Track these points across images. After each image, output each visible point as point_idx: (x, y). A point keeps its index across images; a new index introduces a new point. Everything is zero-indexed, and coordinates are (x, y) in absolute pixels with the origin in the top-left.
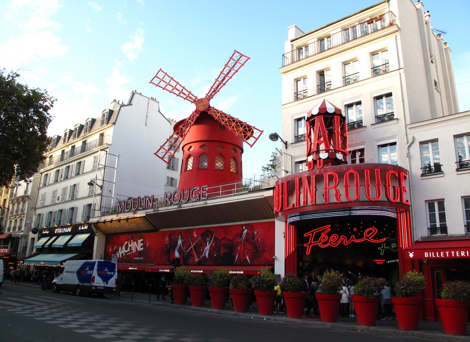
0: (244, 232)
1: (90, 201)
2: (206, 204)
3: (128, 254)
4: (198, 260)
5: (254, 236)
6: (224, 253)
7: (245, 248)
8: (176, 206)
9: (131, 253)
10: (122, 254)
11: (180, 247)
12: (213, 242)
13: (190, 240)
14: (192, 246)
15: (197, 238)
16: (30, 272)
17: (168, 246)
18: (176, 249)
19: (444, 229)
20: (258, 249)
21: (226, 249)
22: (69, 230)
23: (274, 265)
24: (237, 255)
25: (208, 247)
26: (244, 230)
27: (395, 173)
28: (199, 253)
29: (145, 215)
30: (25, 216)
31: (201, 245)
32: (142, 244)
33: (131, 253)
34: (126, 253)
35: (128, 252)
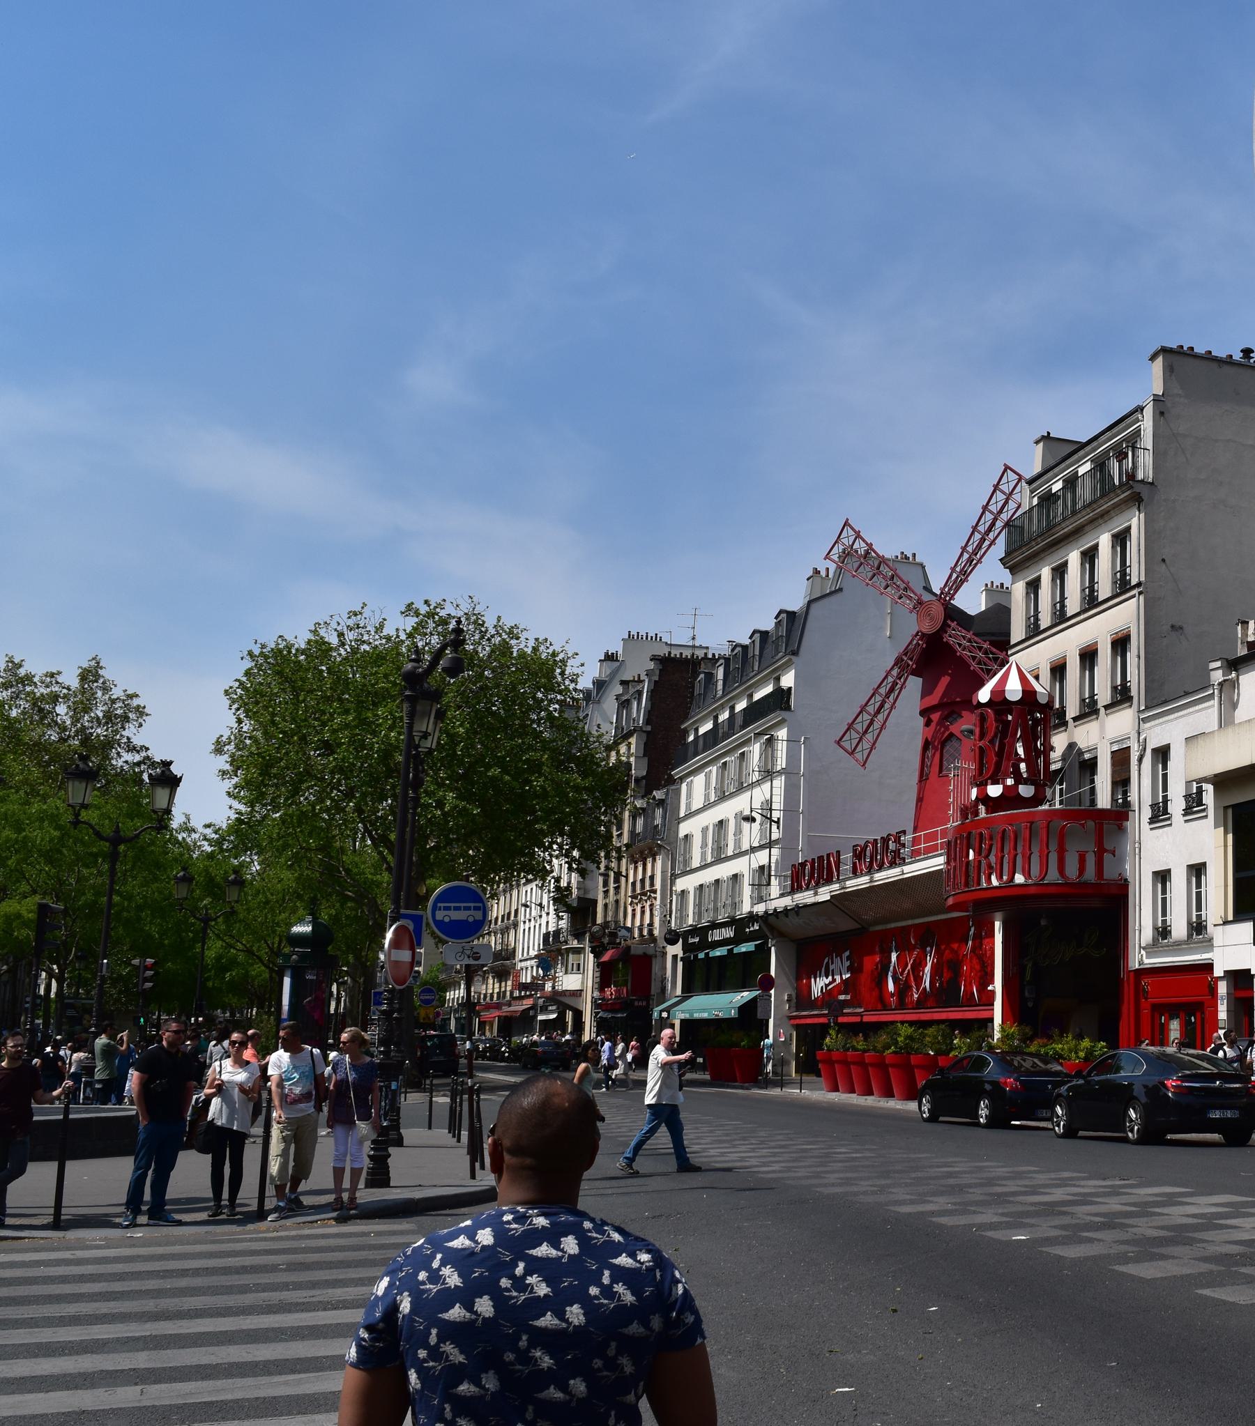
1: (762, 858)
2: (903, 874)
3: (830, 987)
4: (917, 996)
7: (971, 967)
8: (866, 879)
9: (835, 984)
10: (822, 987)
11: (894, 967)
12: (934, 957)
18: (890, 974)
22: (728, 933)
23: (993, 1005)
25: (928, 969)
27: (1080, 824)
28: (919, 980)
29: (829, 898)
30: (658, 895)
32: (848, 963)
33: (835, 984)
34: (827, 985)
35: (830, 983)
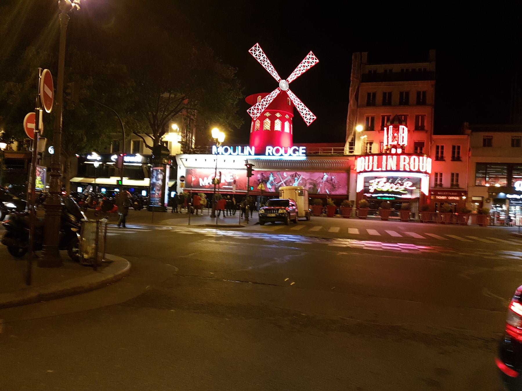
0: (324, 177)
5: (332, 180)
6: (309, 187)
7: (325, 185)
13: (281, 178)
14: (283, 182)
15: (286, 177)
16: (36, 193)
17: (260, 180)
19: (441, 185)
20: (335, 186)
21: (311, 185)
24: (319, 189)
26: (324, 175)
31: (291, 182)
32: (232, 178)
